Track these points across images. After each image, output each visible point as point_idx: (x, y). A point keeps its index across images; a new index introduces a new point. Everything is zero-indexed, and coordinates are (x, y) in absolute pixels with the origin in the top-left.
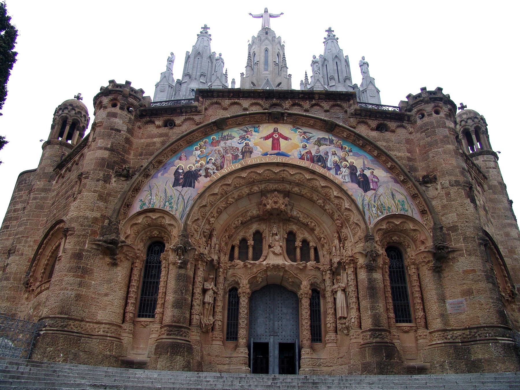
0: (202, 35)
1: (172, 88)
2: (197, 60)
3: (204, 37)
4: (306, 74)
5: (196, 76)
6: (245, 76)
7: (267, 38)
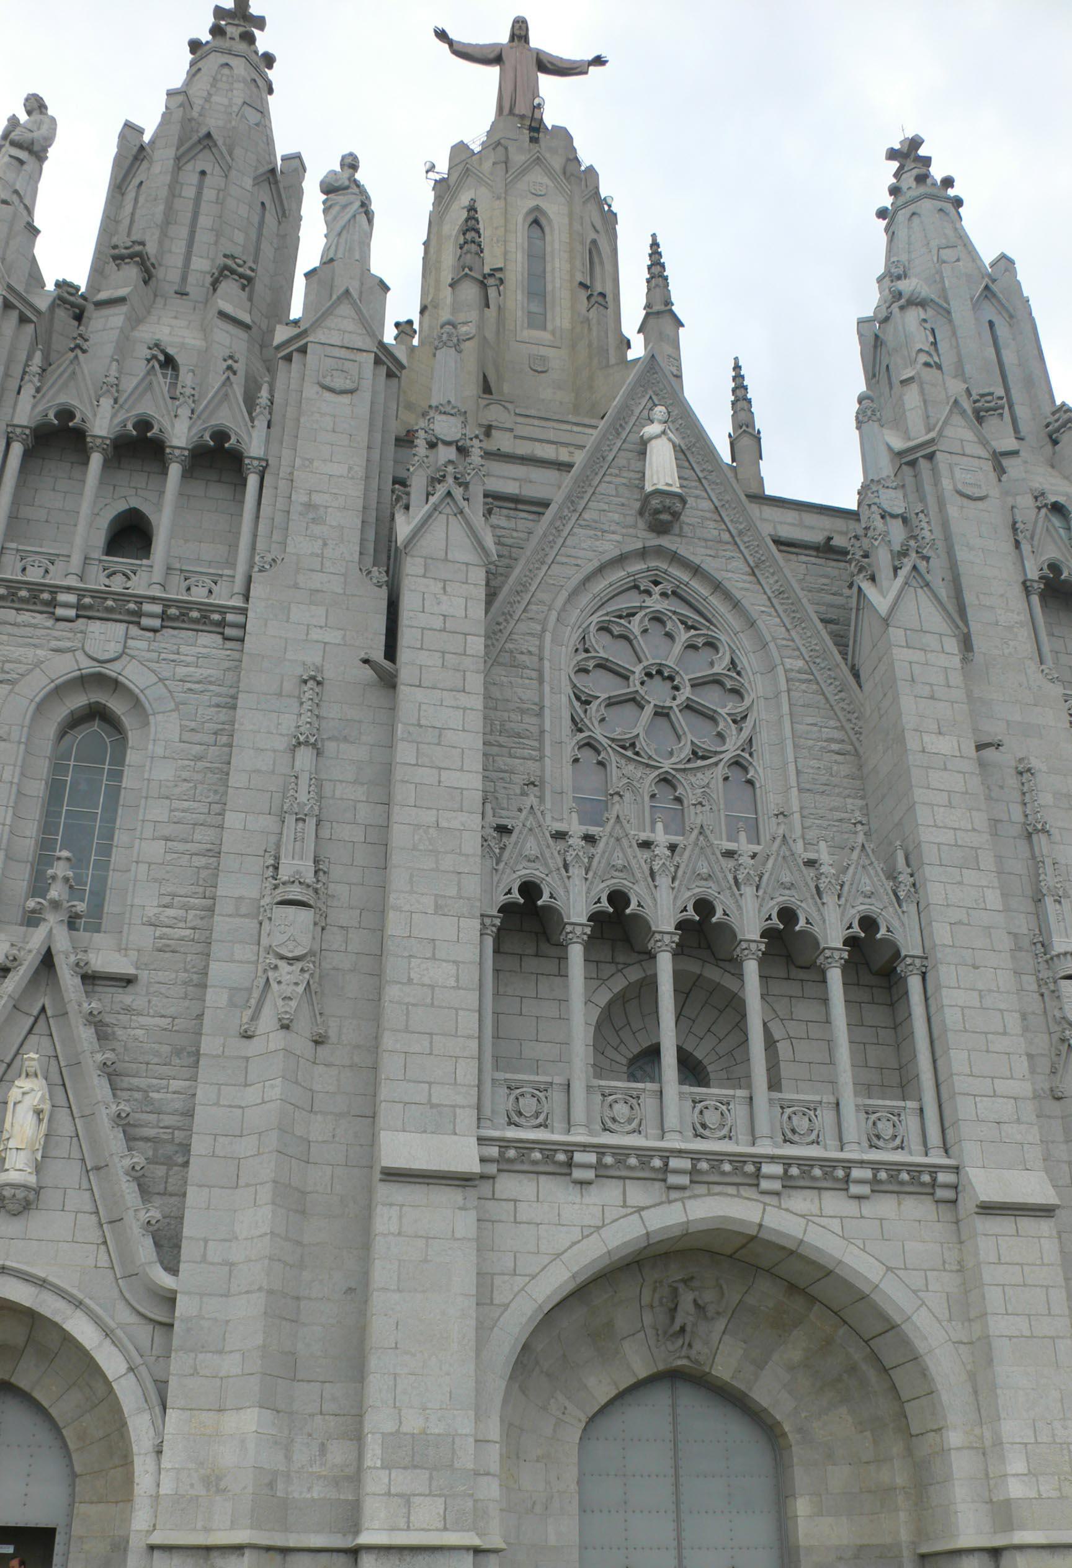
0: (220, 42)
1: (23, 320)
2: (190, 177)
3: (234, 62)
4: (738, 377)
5: (184, 279)
6: (415, 342)
7: (538, 161)
